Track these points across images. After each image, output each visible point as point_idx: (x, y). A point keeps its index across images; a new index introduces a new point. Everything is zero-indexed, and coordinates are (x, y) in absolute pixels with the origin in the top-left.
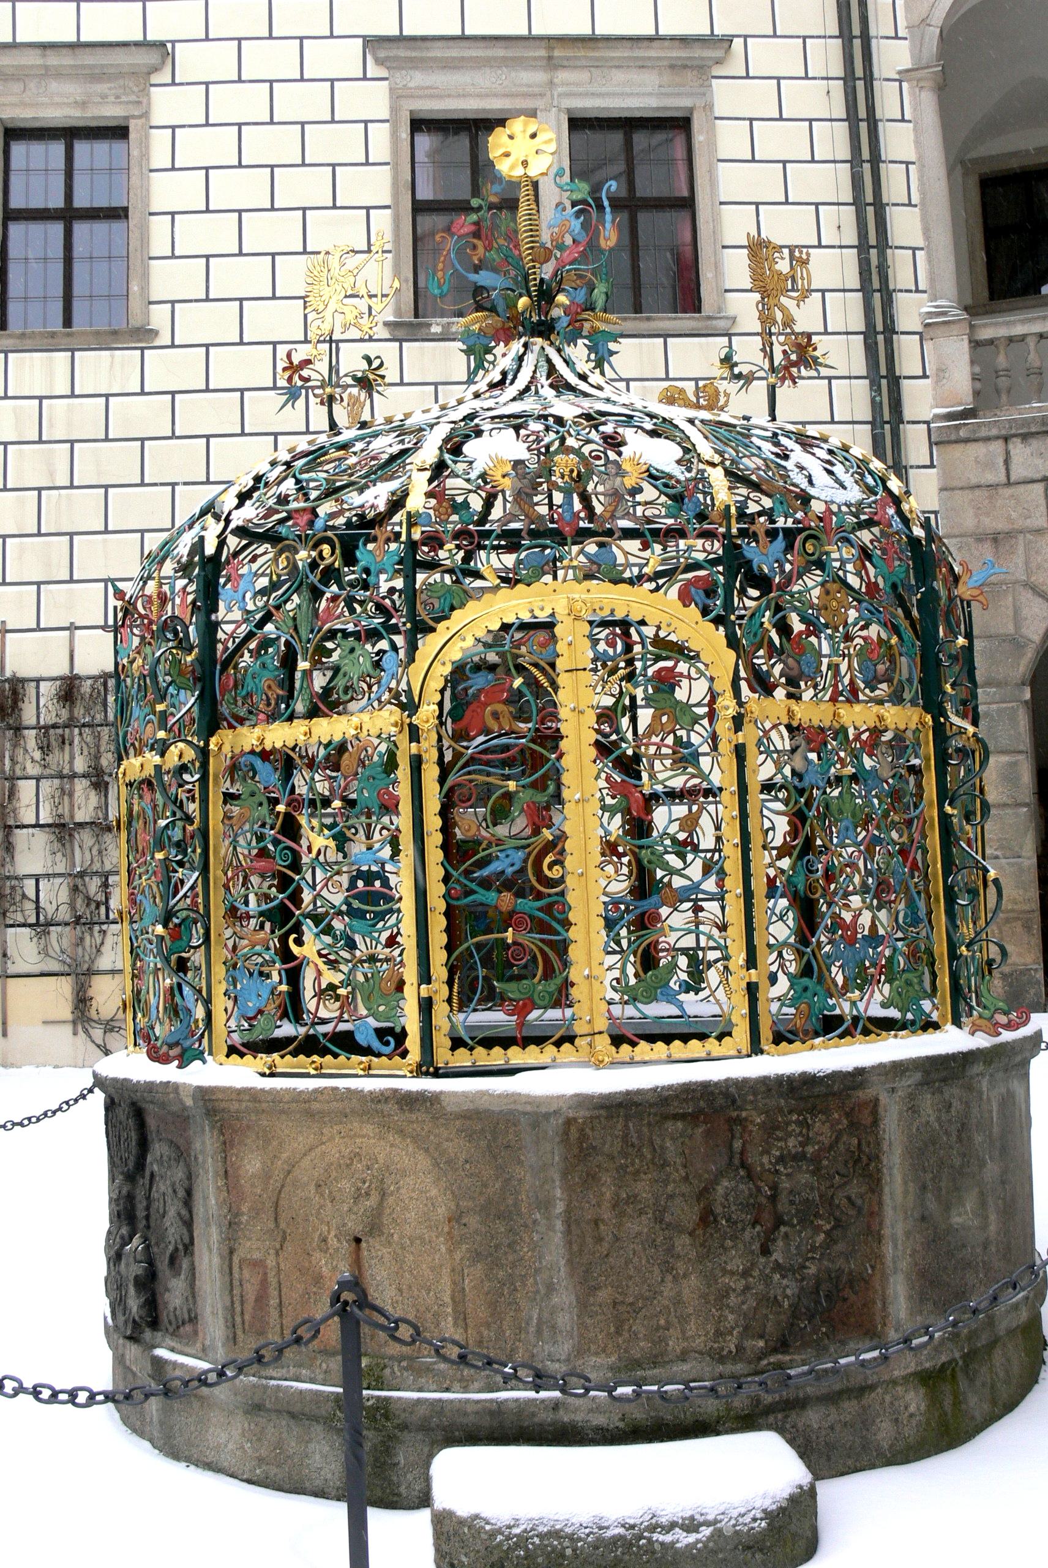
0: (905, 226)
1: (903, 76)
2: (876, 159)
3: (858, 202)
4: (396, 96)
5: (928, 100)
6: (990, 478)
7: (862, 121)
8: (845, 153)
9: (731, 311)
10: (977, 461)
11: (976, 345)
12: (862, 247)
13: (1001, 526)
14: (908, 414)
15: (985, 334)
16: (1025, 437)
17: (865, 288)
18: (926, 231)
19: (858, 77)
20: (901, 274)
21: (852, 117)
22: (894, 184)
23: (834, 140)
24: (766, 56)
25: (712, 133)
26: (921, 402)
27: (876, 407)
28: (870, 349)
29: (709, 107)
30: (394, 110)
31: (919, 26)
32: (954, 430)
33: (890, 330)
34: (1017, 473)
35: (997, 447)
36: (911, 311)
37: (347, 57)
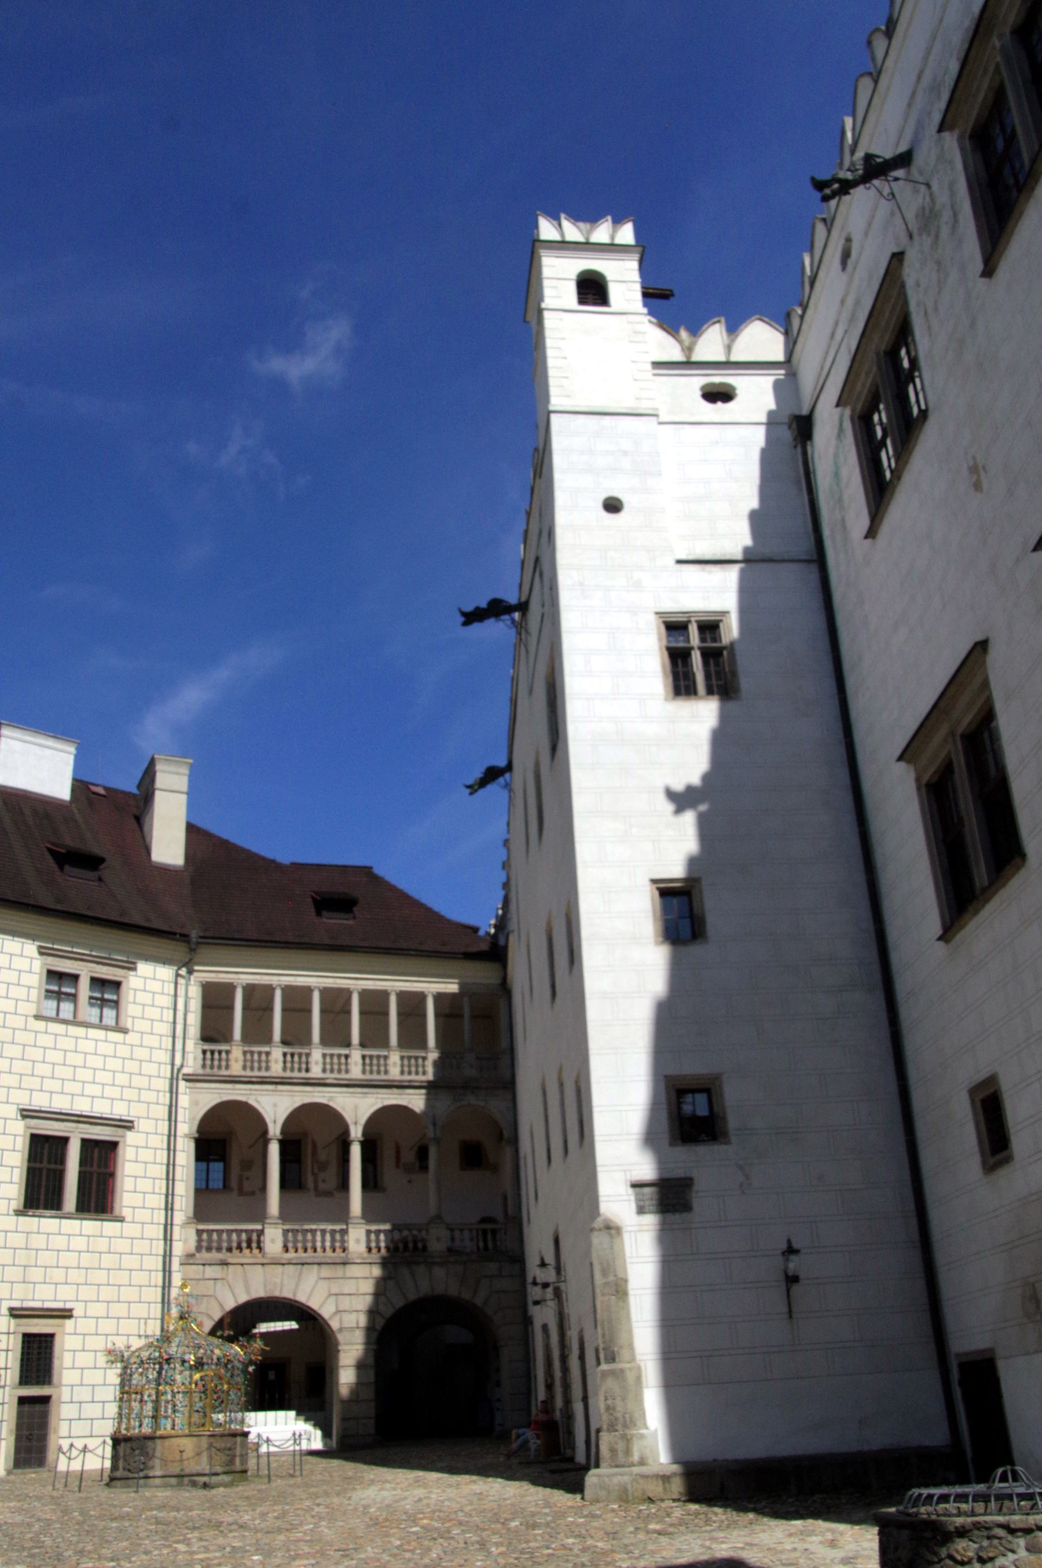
1: (186, 1136)
4: (28, 1127)
6: (198, 1277)
7: (171, 1149)
9: (124, 1214)
10: (194, 1271)
13: (199, 1293)
14: (174, 1253)
15: (201, 1227)
16: (210, 1264)
18: (187, 1191)
19: (172, 1135)
22: (179, 1175)
23: (162, 1156)
24: (142, 1125)
25: (124, 1150)
26: (179, 1249)
27: (165, 1251)
29: (125, 1142)
30: (25, 1132)
31: (192, 1119)
32: (188, 1259)
34: (207, 1276)
35: (201, 1267)
36: (179, 1217)
37: (12, 1111)
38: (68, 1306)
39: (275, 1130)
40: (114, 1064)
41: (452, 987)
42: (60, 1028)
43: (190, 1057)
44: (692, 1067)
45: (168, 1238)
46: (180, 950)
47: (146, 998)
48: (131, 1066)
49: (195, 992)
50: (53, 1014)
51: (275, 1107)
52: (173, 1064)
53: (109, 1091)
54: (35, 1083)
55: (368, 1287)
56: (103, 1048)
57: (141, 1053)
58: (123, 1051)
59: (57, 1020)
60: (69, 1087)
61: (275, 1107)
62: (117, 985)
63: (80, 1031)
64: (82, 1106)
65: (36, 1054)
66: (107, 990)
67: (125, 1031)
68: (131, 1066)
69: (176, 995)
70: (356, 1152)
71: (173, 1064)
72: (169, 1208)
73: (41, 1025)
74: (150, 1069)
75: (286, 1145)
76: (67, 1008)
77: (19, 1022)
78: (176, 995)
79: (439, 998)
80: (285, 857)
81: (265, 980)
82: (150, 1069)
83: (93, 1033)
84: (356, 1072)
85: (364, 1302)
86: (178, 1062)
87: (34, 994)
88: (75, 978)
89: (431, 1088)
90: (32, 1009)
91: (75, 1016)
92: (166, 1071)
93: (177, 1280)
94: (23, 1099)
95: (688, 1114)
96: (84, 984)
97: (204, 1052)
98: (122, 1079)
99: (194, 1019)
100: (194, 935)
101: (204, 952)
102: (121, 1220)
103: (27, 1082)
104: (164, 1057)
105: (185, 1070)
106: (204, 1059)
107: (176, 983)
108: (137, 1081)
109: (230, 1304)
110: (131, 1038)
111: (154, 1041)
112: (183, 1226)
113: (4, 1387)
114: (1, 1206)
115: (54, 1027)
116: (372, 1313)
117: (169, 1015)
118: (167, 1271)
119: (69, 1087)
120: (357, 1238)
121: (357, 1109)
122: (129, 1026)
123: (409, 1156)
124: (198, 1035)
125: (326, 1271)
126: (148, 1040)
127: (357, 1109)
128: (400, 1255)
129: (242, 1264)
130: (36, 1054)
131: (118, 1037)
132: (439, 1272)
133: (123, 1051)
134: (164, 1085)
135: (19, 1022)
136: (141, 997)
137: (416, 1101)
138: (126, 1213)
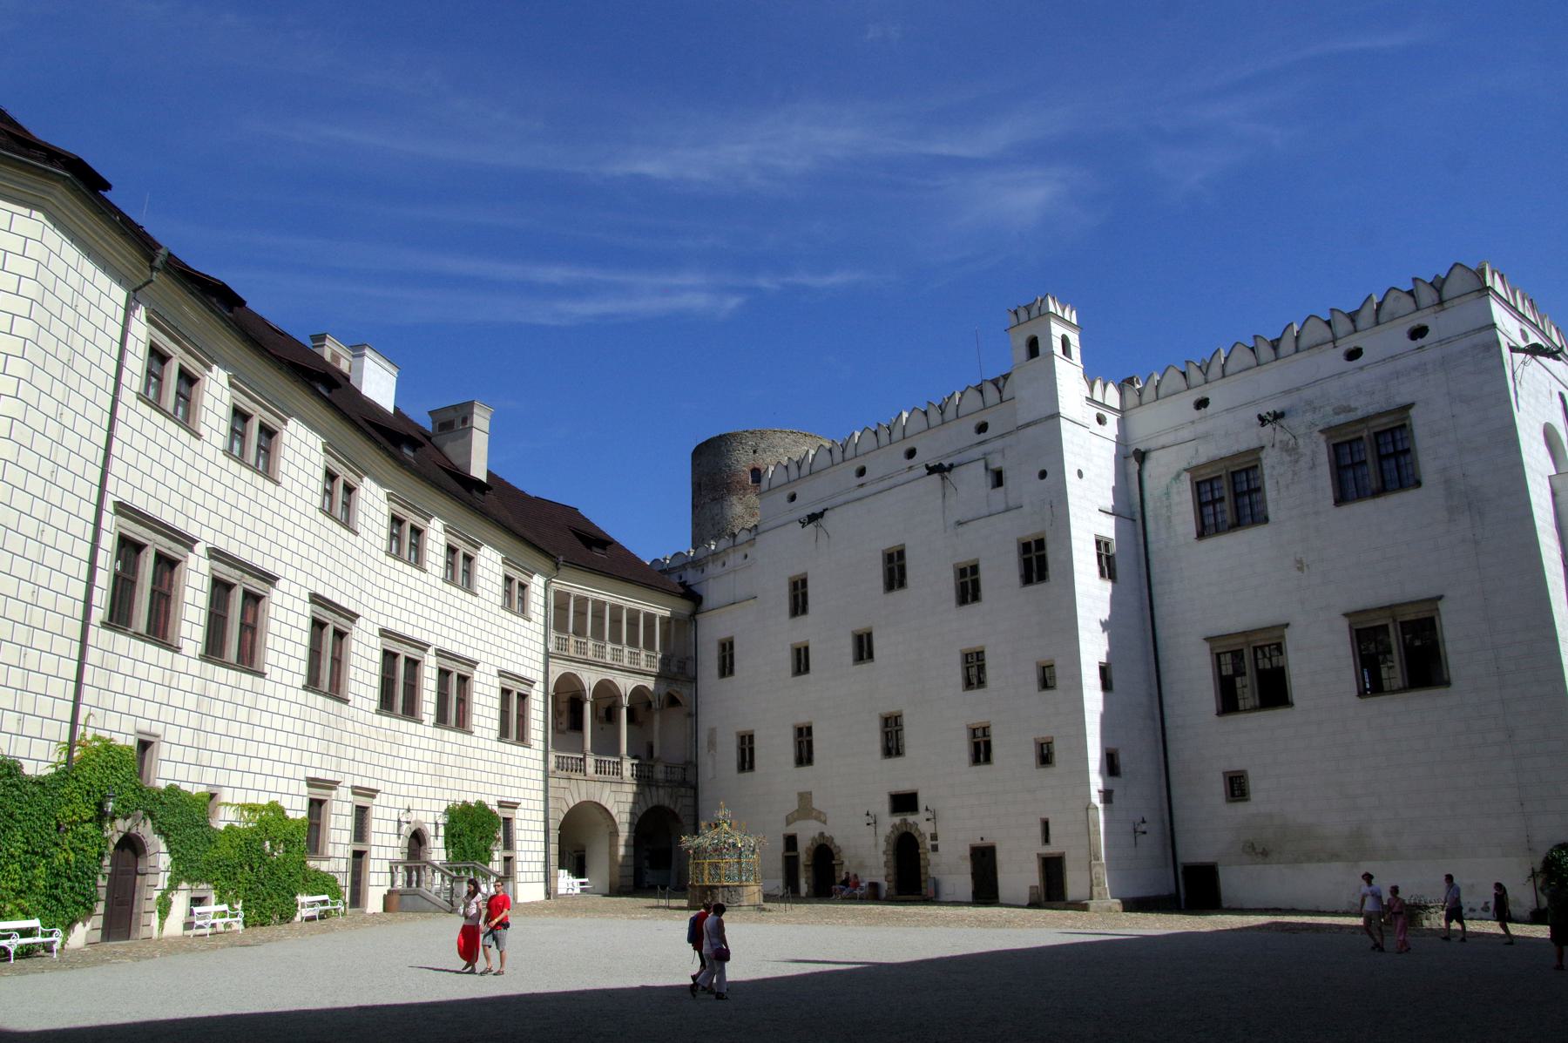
39: (589, 695)
41: (668, 614)
44: (1112, 746)
45: (546, 760)
46: (547, 564)
51: (590, 678)
55: (630, 798)
61: (590, 678)
70: (588, 707)
75: (629, 710)
79: (662, 618)
80: (532, 490)
81: (586, 594)
84: (626, 663)
85: (627, 808)
89: (658, 677)
92: (541, 649)
95: (1111, 765)
101: (564, 571)
104: (541, 639)
116: (632, 813)
120: (627, 766)
121: (626, 684)
123: (602, 713)
125: (614, 787)
127: (626, 684)
128: (644, 779)
132: (661, 792)
134: (541, 658)
137: (650, 683)
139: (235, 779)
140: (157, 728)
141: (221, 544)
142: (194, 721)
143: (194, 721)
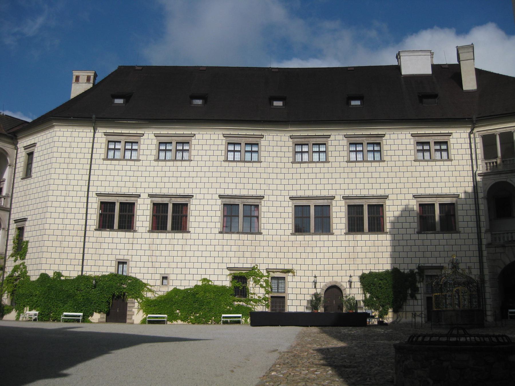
0: (483, 218)
1: (482, 198)
2: (479, 209)
3: (476, 216)
4: (417, 202)
5: (486, 201)
8: (474, 209)
11: (492, 234)
12: (477, 221)
17: (477, 227)
20: (482, 224)
21: (475, 204)
22: (481, 213)
26: (484, 242)
27: (479, 243)
28: (478, 235)
32: (489, 245)
33: (480, 232)
36: (483, 230)
37: (411, 196)
38: (442, 265)
40: (448, 174)
42: (425, 163)
43: (480, 167)
45: (480, 239)
47: (459, 146)
48: (456, 174)
49: (479, 140)
50: (422, 159)
52: (473, 170)
53: (448, 185)
54: (418, 185)
56: (443, 168)
57: (458, 168)
58: (452, 168)
59: (424, 160)
60: (432, 185)
62: (446, 143)
63: (433, 163)
64: (438, 191)
65: (417, 174)
66: (443, 145)
67: (451, 160)
68: (456, 174)
69: (470, 143)
71: (473, 170)
72: (479, 227)
73: (417, 163)
74: (463, 174)
76: (427, 155)
77: (409, 164)
78: (470, 143)
82: (463, 174)
83: (438, 163)
86: (475, 169)
87: (413, 152)
88: (428, 143)
90: (413, 158)
91: (424, 158)
92: (470, 173)
93: (485, 253)
94: (415, 192)
96: (432, 144)
97: (486, 163)
98: (453, 179)
99: (480, 151)
100: (474, 118)
102: (459, 232)
103: (415, 185)
105: (478, 172)
106: (487, 167)
107: (470, 138)
108: (459, 179)
109: (508, 262)
110: (454, 163)
111: (464, 162)
112: (486, 232)
113: (421, 293)
114: (411, 231)
115: (422, 163)
117: (469, 151)
118: (480, 251)
119: (432, 185)
122: (453, 158)
124: (483, 158)
126: (461, 163)
129: (511, 246)
130: (417, 174)
131: (449, 163)
133: (452, 168)
135: (409, 164)
136: (456, 146)
138: (461, 230)
139: (178, 271)
140: (126, 257)
141: (150, 191)
142: (148, 253)
143: (148, 253)
